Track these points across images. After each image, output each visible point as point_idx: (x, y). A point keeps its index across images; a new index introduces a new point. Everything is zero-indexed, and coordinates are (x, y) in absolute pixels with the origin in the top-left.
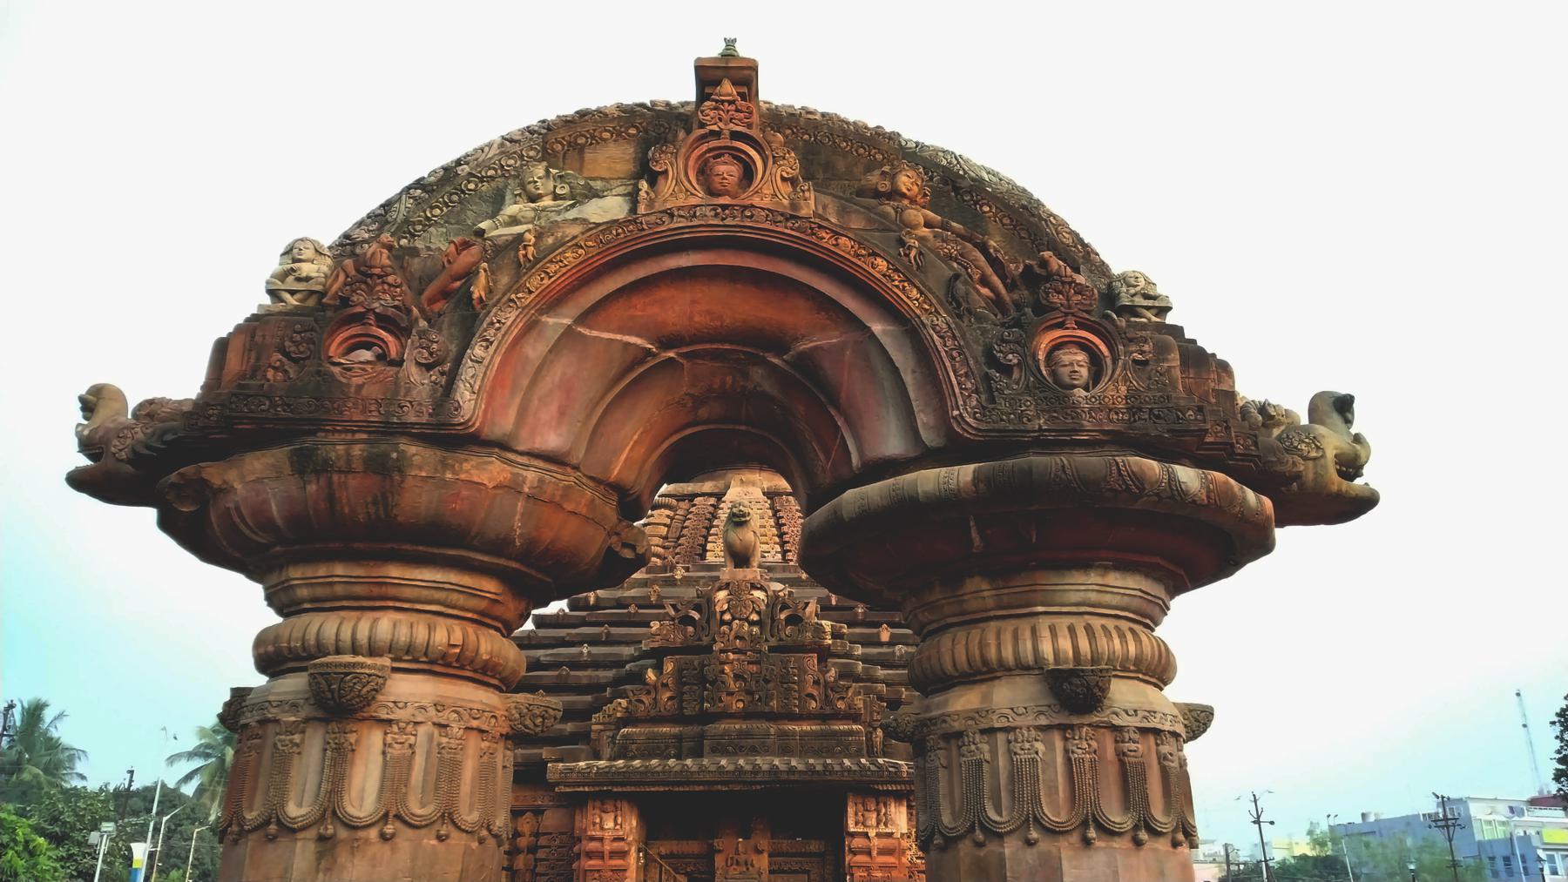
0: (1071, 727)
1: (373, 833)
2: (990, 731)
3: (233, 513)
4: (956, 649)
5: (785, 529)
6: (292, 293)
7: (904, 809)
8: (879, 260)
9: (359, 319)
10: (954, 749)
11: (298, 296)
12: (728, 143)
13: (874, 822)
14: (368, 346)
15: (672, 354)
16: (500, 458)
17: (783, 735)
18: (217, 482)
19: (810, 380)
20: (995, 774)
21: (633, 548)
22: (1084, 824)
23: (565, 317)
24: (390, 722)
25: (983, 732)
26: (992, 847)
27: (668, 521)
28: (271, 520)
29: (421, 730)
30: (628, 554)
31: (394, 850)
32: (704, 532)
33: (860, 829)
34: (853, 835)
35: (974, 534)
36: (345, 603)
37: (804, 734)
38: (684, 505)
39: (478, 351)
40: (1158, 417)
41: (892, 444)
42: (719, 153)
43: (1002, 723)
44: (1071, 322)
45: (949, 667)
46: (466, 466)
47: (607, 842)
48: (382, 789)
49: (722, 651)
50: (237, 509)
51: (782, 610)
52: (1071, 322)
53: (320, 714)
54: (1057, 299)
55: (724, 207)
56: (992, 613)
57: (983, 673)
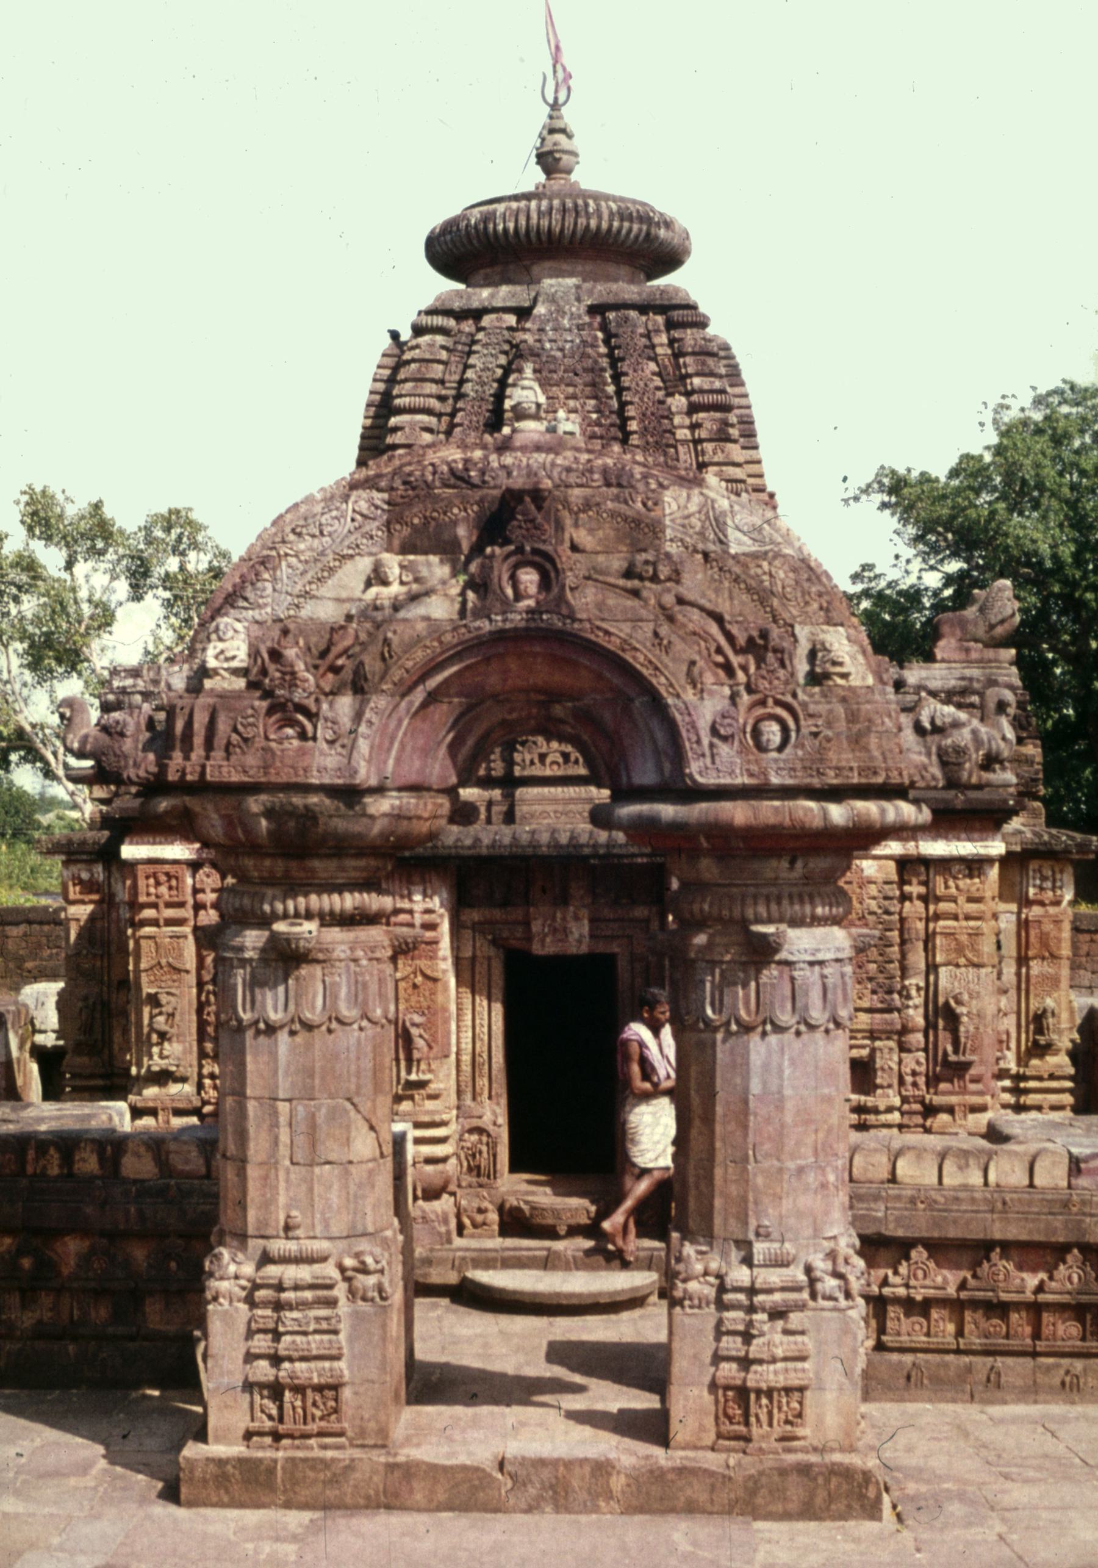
14: (292, 726)
22: (764, 1023)
24: (324, 961)
25: (708, 962)
27: (444, 355)
38: (468, 326)
44: (770, 701)
47: (417, 916)
52: (770, 701)
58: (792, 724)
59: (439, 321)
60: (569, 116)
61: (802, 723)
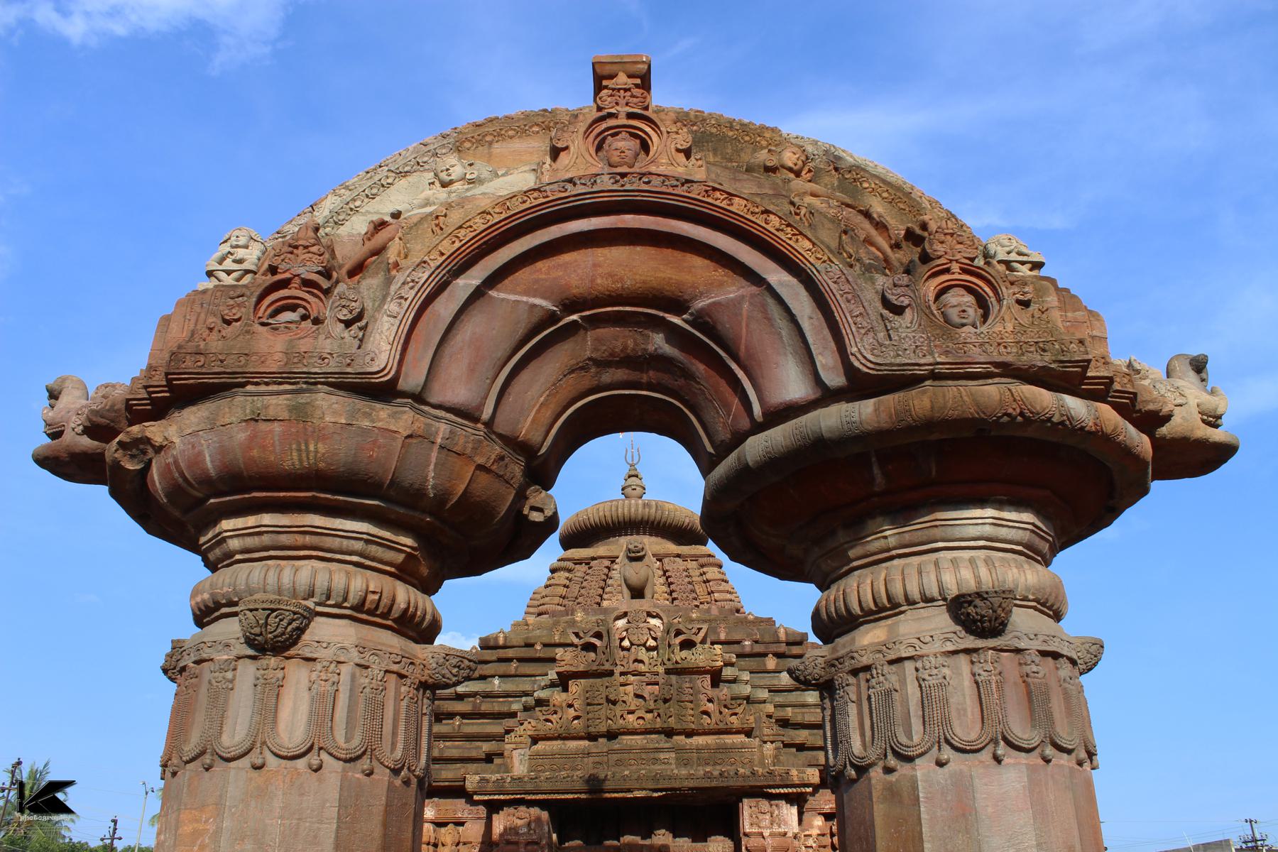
0: (976, 650)
1: (301, 763)
2: (899, 660)
3: (173, 468)
4: (860, 588)
5: (673, 587)
6: (229, 273)
7: (794, 810)
8: (772, 217)
9: (284, 284)
10: (863, 683)
11: (235, 275)
12: (625, 122)
13: (767, 822)
14: (293, 308)
15: (575, 317)
16: (412, 408)
17: (678, 750)
18: (158, 439)
19: (711, 343)
20: (905, 702)
21: (541, 510)
22: (994, 741)
23: (474, 278)
24: (314, 660)
25: (891, 662)
26: (903, 769)
28: (205, 470)
29: (345, 669)
30: (536, 517)
31: (320, 780)
32: (600, 591)
33: (755, 830)
34: (746, 835)
35: (876, 471)
36: (272, 553)
37: (699, 749)
38: (584, 568)
39: (392, 307)
40: (1044, 350)
41: (791, 384)
42: (615, 132)
43: (911, 652)
44: (955, 267)
45: (856, 609)
46: (383, 414)
48: (309, 723)
49: (622, 674)
50: (176, 462)
51: (676, 636)
52: (955, 267)
53: (251, 652)
54: (940, 249)
55: (623, 175)
56: (894, 552)
57: (887, 609)
58: (987, 289)
59: (563, 564)
60: (640, 470)
61: (1005, 291)
